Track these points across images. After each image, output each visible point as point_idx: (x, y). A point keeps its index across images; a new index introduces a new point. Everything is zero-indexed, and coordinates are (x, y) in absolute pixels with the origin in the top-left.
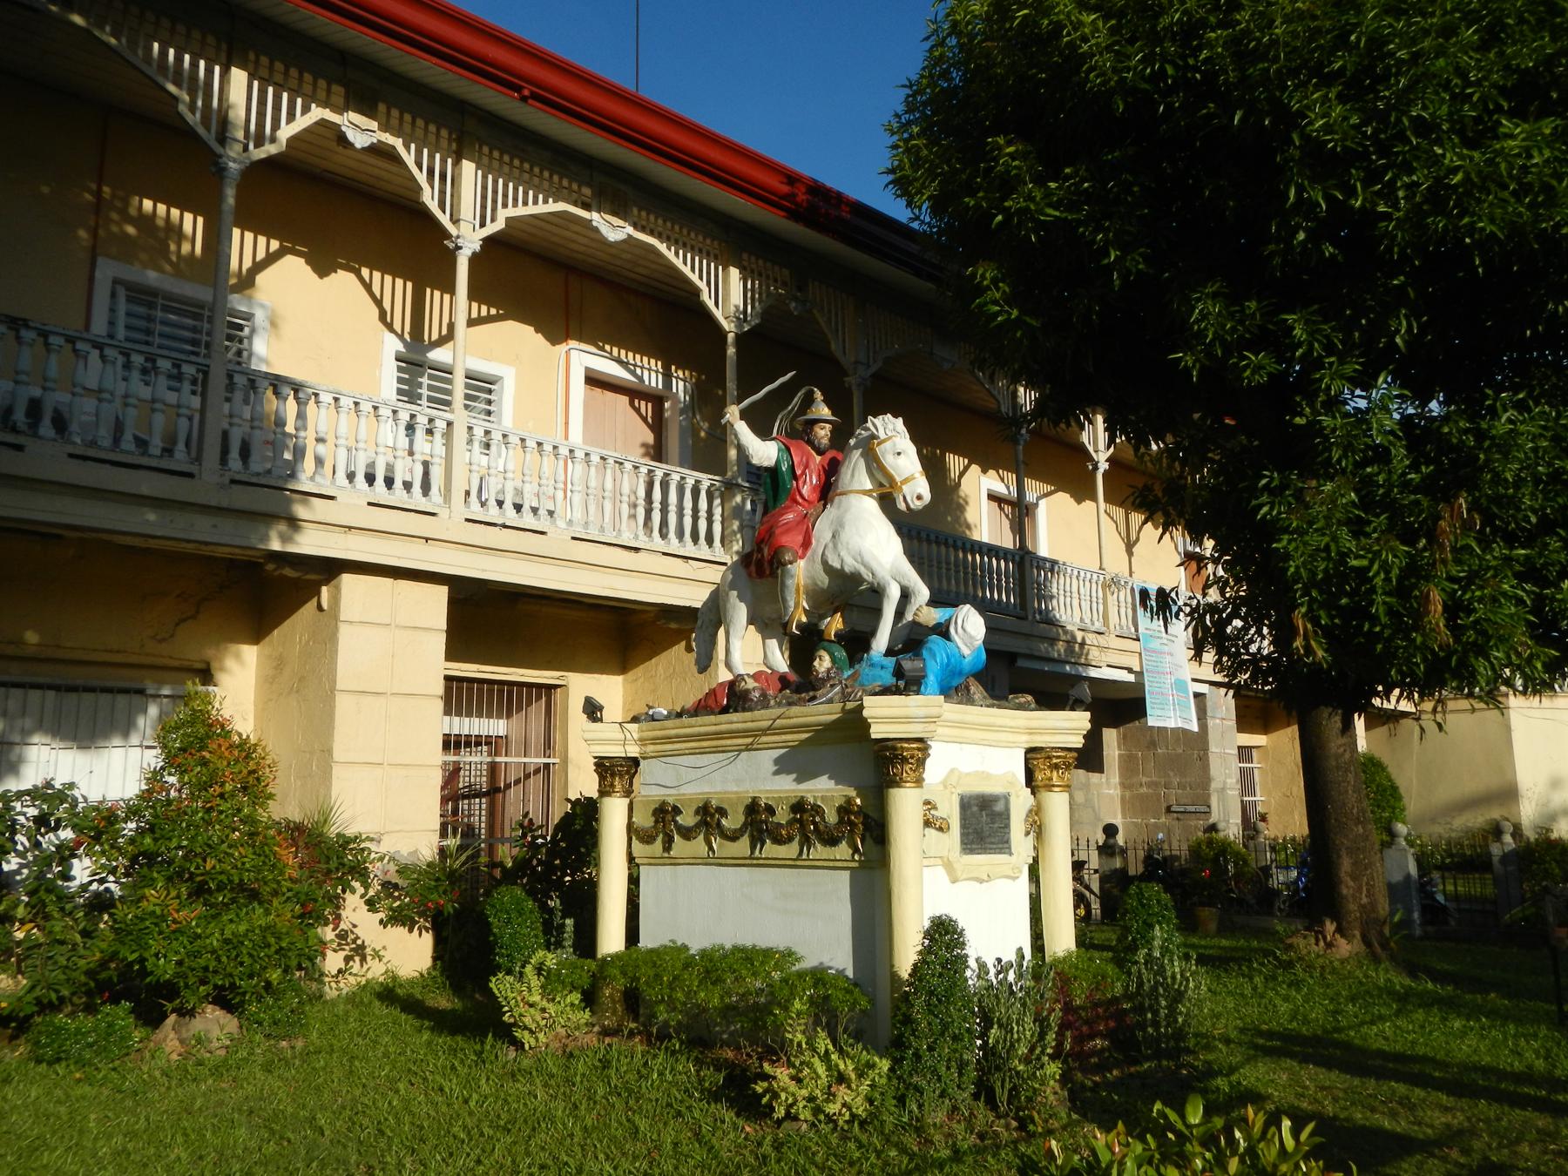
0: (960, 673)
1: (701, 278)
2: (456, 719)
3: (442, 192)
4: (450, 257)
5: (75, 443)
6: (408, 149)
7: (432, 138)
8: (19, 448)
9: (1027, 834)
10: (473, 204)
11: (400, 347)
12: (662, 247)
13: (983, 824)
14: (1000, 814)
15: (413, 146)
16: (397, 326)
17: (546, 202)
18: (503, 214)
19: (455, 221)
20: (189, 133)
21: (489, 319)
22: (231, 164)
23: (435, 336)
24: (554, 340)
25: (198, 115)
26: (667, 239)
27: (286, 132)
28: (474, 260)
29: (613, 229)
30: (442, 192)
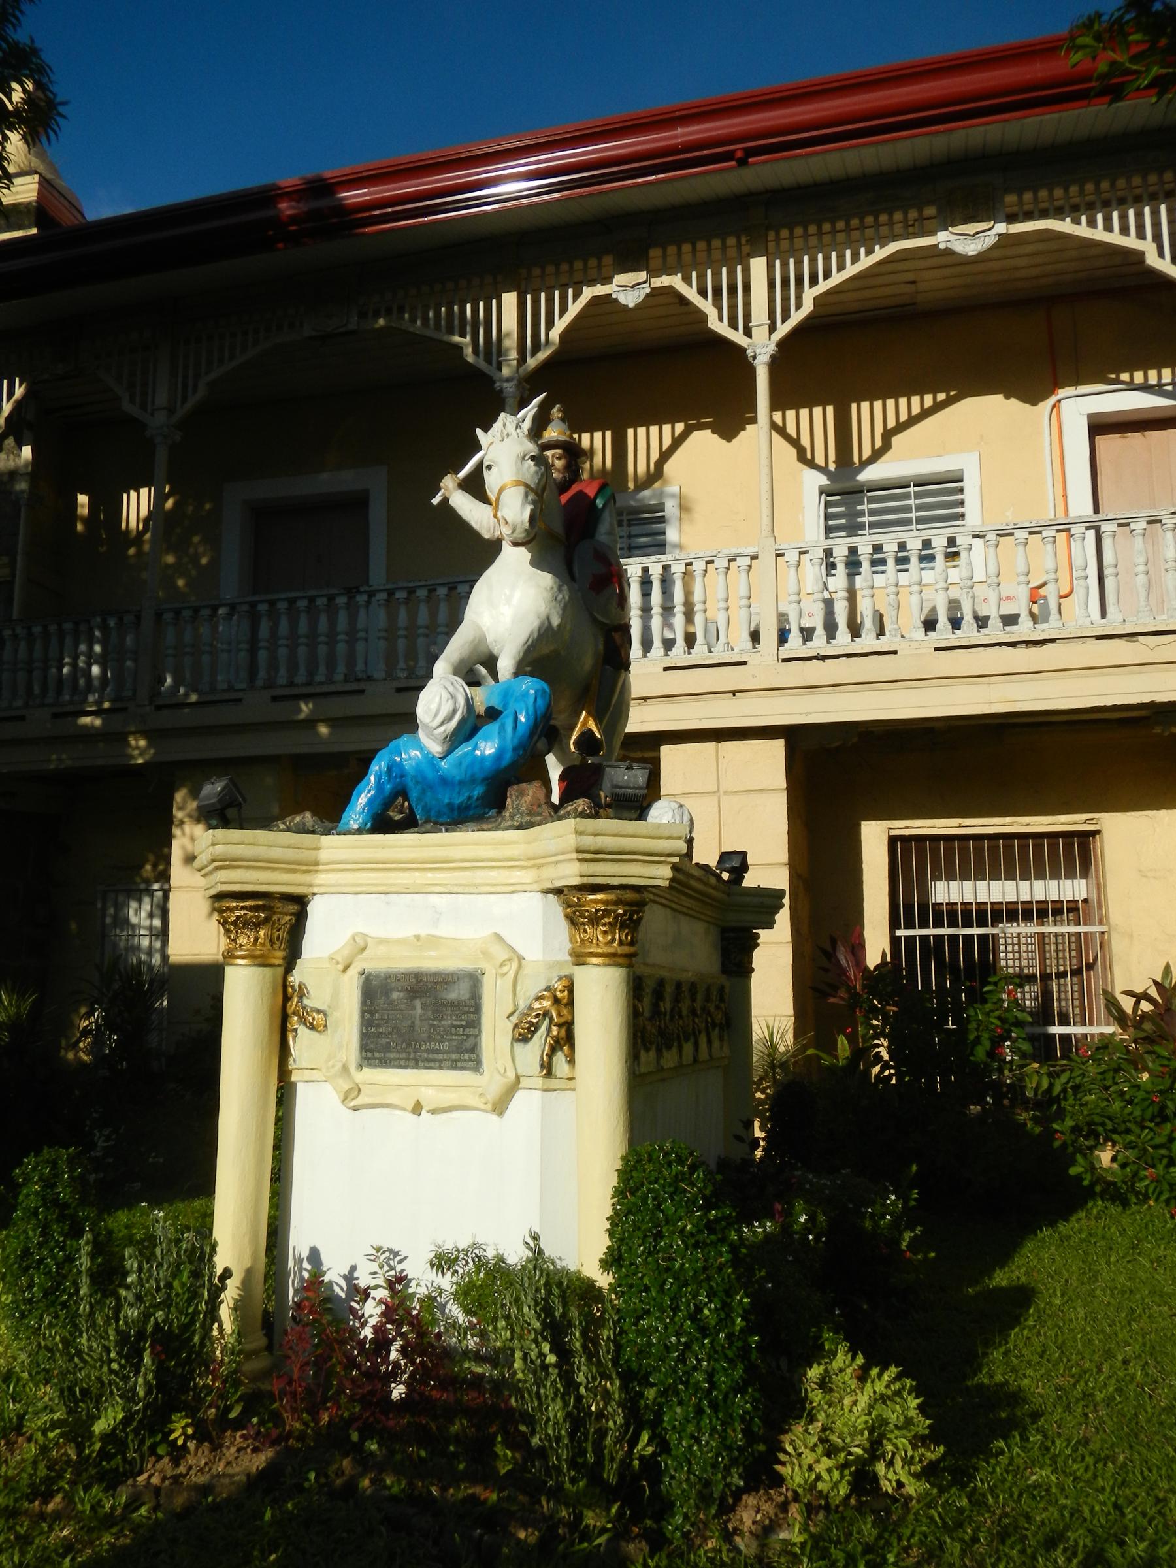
0: (444, 781)
1: (1141, 235)
2: (1054, 883)
3: (733, 307)
4: (751, 371)
5: (399, 678)
6: (687, 280)
7: (717, 255)
8: (362, 692)
9: (524, 1039)
10: (758, 305)
11: (823, 480)
12: (1064, 226)
13: (418, 1020)
14: (456, 1005)
15: (694, 274)
16: (820, 460)
17: (855, 258)
18: (810, 295)
19: (748, 333)
20: (474, 373)
21: (938, 407)
22: (505, 385)
23: (867, 453)
24: (1033, 397)
25: (482, 355)
26: (1073, 211)
27: (560, 325)
28: (775, 364)
29: (969, 240)
30: (733, 307)
